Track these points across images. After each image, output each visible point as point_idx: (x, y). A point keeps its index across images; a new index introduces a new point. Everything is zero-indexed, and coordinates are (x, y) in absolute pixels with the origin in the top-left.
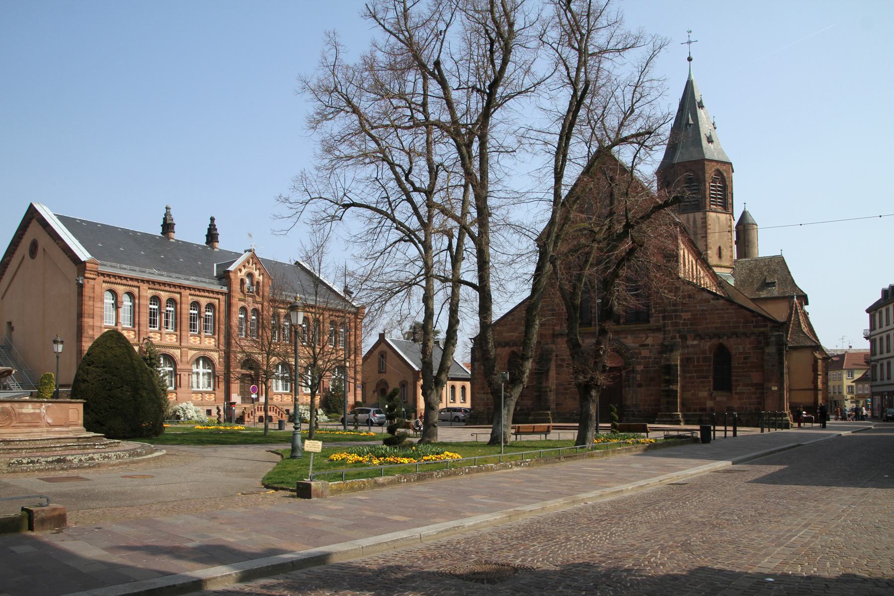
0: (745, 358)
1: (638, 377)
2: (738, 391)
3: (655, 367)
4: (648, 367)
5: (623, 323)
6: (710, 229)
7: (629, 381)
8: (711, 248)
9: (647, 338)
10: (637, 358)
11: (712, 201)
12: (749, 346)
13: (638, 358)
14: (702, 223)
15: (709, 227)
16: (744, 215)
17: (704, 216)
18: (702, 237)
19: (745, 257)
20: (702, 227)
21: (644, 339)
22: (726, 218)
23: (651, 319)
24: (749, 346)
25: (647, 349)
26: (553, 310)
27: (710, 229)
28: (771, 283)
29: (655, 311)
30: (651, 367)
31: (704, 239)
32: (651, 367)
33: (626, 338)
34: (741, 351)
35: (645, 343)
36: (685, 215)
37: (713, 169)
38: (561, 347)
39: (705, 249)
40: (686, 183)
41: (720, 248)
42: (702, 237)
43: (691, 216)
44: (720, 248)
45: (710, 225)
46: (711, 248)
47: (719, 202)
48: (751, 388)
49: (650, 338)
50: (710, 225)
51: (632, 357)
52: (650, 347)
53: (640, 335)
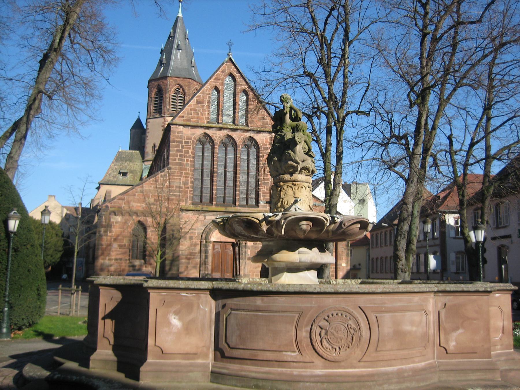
1: (249, 252)
26: (180, 187)
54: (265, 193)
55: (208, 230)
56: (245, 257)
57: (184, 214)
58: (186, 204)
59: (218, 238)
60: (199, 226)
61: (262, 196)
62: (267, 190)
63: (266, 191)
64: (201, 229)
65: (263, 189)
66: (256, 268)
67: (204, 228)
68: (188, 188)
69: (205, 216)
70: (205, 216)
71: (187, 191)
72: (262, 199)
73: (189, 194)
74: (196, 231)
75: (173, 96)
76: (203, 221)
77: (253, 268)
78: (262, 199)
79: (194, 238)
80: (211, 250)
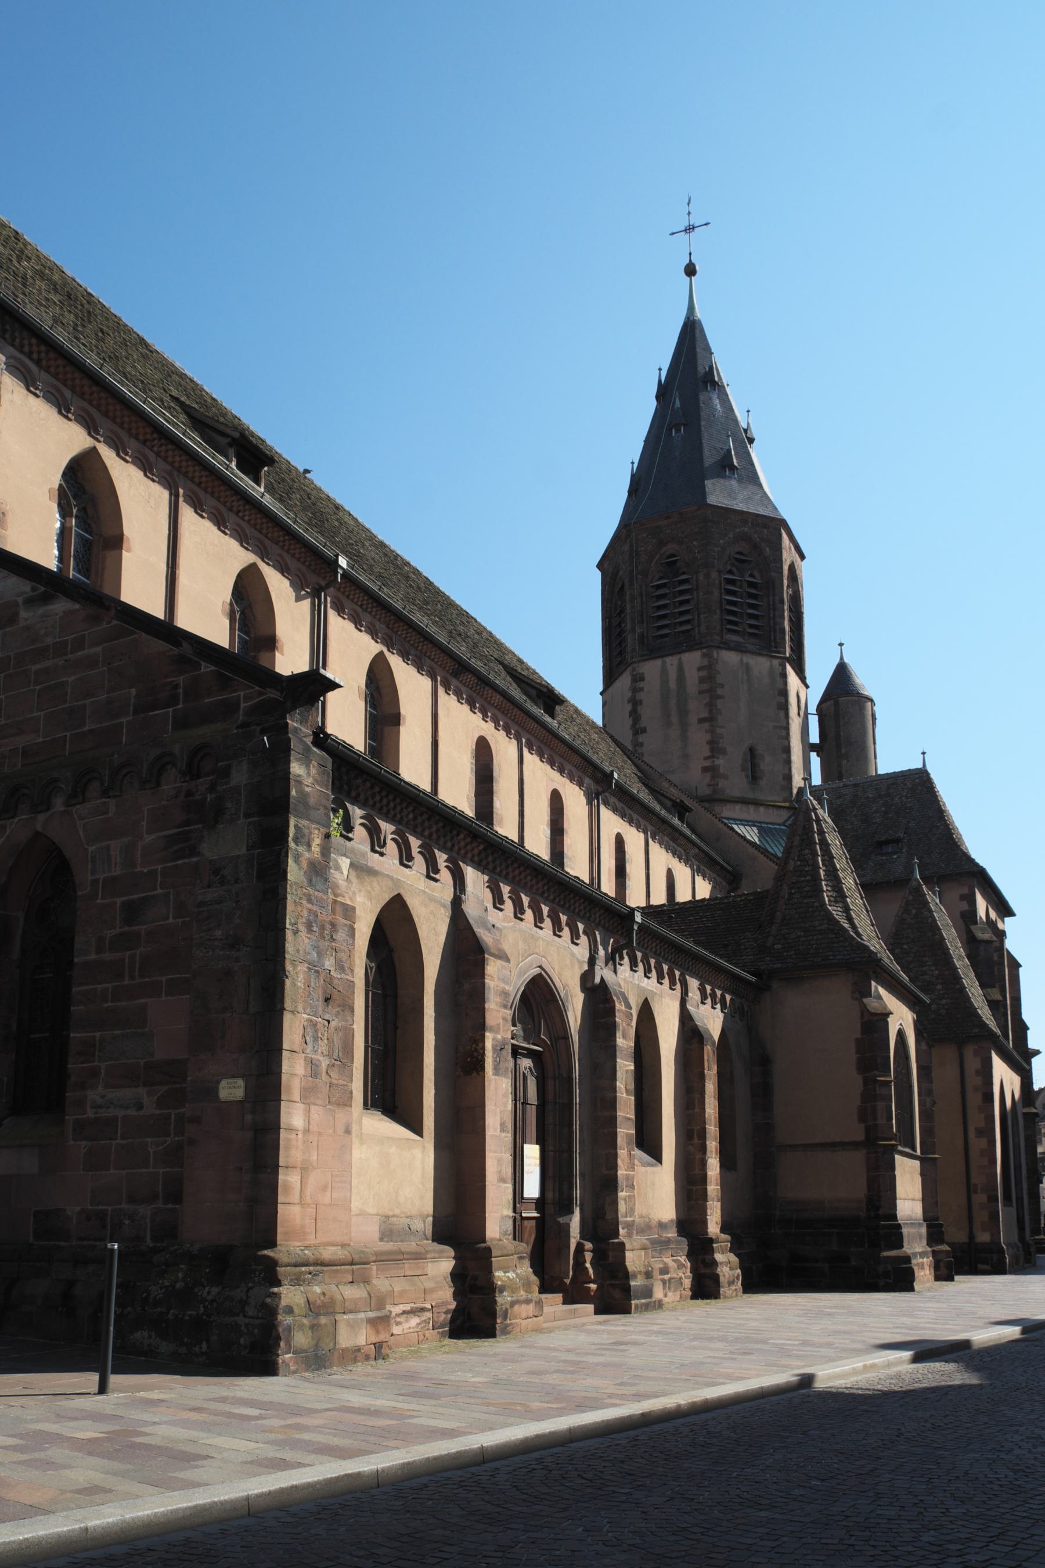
0: (132, 912)
2: (90, 1114)
6: (721, 697)
8: (724, 752)
11: (730, 622)
12: (149, 838)
14: (702, 680)
15: (719, 691)
16: (842, 676)
17: (706, 662)
18: (701, 721)
19: (840, 777)
20: (701, 692)
22: (771, 671)
24: (149, 838)
27: (721, 697)
28: (887, 842)
31: (706, 725)
34: (117, 872)
36: (658, 662)
37: (731, 535)
39: (708, 754)
40: (661, 578)
41: (752, 750)
42: (701, 721)
43: (672, 662)
44: (752, 750)
45: (722, 686)
46: (724, 752)
47: (751, 626)
48: (142, 1091)
50: (722, 686)
75: (659, 587)
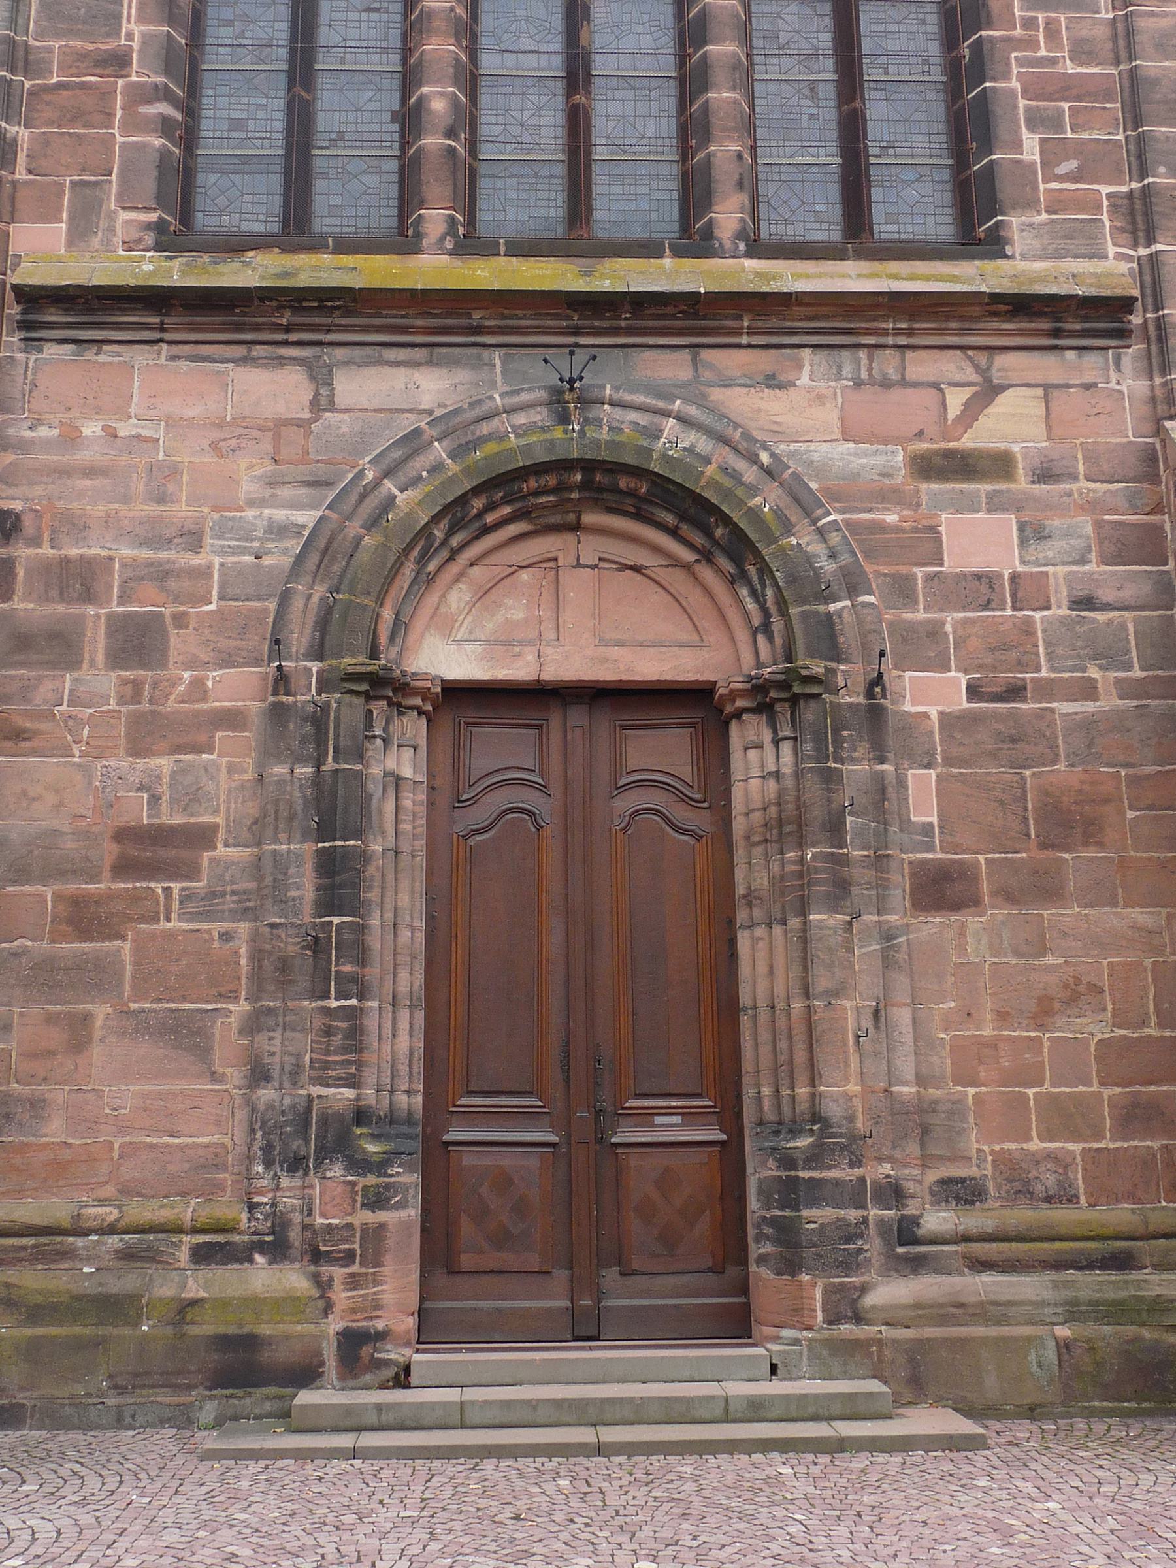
3: (1089, 691)
4: (1015, 692)
5: (741, 235)
7: (835, 829)
9: (990, 391)
10: (903, 590)
13: (903, 590)
21: (956, 400)
23: (1014, 221)
25: (995, 504)
29: (1052, 152)
30: (1047, 690)
32: (1047, 690)
33: (772, 382)
35: (967, 442)
38: (71, 438)
49: (1005, 402)
51: (853, 584)
52: (1022, 483)
53: (922, 366)
54: (1066, 88)
55: (354, 528)
56: (880, 861)
57: (52, 351)
58: (80, 232)
59: (504, 643)
60: (248, 487)
61: (1034, 122)
62: (1082, 51)
63: (1071, 68)
64: (280, 531)
65: (1033, 44)
66: (1043, 1013)
67: (308, 518)
68: (119, 61)
69: (322, 378)
70: (322, 378)
71: (107, 95)
72: (1031, 146)
73: (132, 124)
74: (211, 557)
76: (299, 423)
77: (1002, 1016)
78: (1031, 146)
79: (175, 640)
80: (416, 800)
